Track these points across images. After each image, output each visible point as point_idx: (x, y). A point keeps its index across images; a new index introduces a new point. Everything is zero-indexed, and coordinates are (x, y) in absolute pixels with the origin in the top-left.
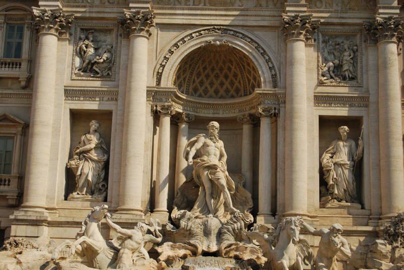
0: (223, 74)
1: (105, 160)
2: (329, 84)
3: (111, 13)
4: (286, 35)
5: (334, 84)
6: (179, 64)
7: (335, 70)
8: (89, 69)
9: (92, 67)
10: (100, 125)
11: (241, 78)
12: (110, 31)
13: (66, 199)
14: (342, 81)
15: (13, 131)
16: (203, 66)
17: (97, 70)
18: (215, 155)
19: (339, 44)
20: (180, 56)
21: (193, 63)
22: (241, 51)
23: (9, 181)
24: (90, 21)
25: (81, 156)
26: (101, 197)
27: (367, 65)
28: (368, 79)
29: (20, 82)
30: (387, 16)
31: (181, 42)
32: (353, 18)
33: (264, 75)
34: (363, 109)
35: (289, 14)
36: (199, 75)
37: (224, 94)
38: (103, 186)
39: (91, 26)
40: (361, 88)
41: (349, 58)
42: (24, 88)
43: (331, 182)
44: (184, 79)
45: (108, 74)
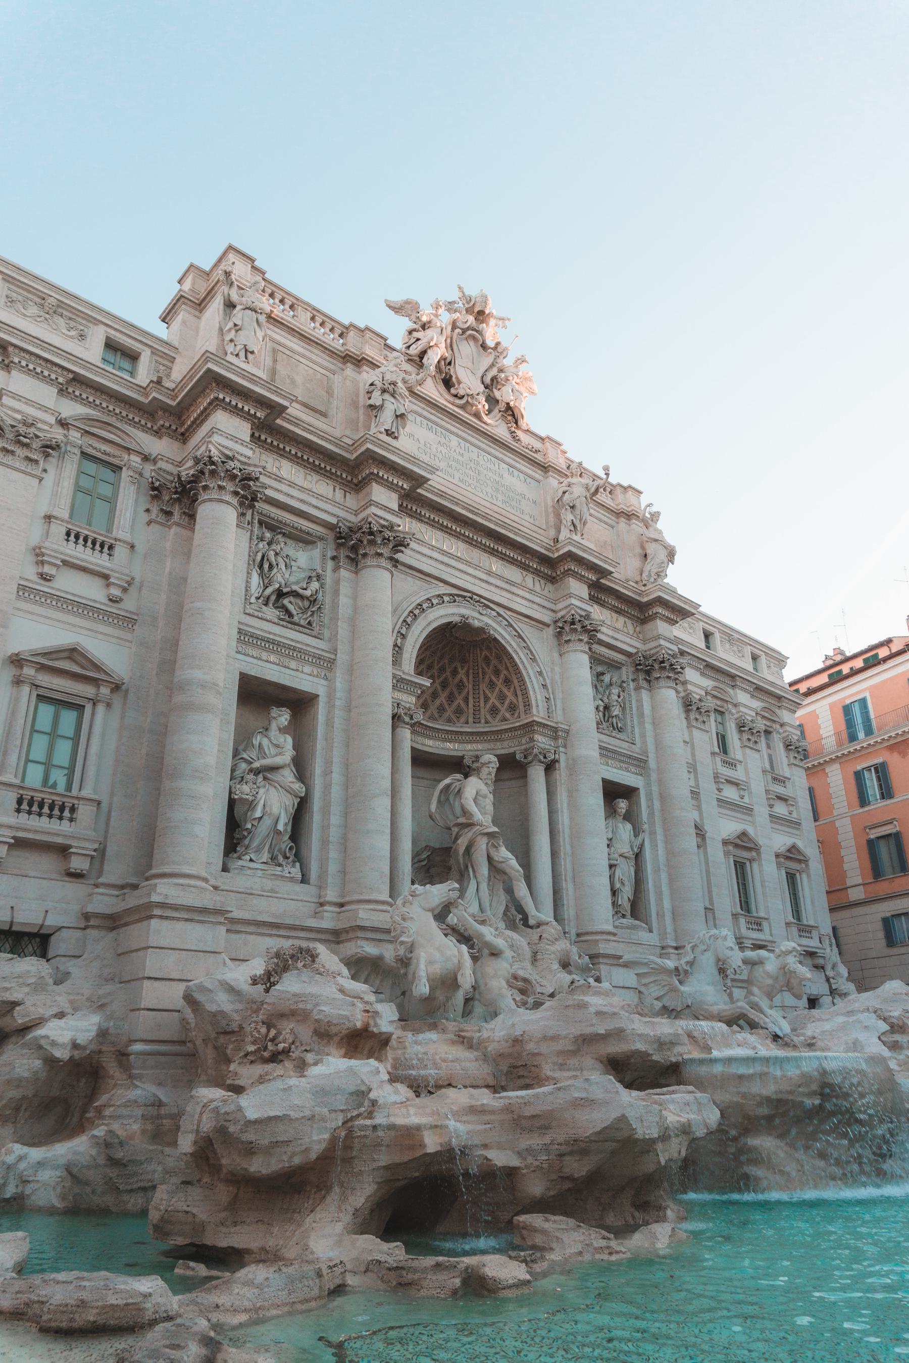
1: (303, 795)
13: (225, 869)
15: (89, 690)
17: (291, 608)
19: (603, 674)
22: (503, 646)
23: (73, 809)
25: (260, 777)
26: (296, 871)
27: (641, 715)
28: (643, 736)
29: (108, 585)
30: (670, 652)
32: (624, 643)
33: (536, 695)
34: (639, 777)
38: (291, 848)
39: (281, 522)
41: (620, 700)
42: (113, 600)
45: (310, 623)
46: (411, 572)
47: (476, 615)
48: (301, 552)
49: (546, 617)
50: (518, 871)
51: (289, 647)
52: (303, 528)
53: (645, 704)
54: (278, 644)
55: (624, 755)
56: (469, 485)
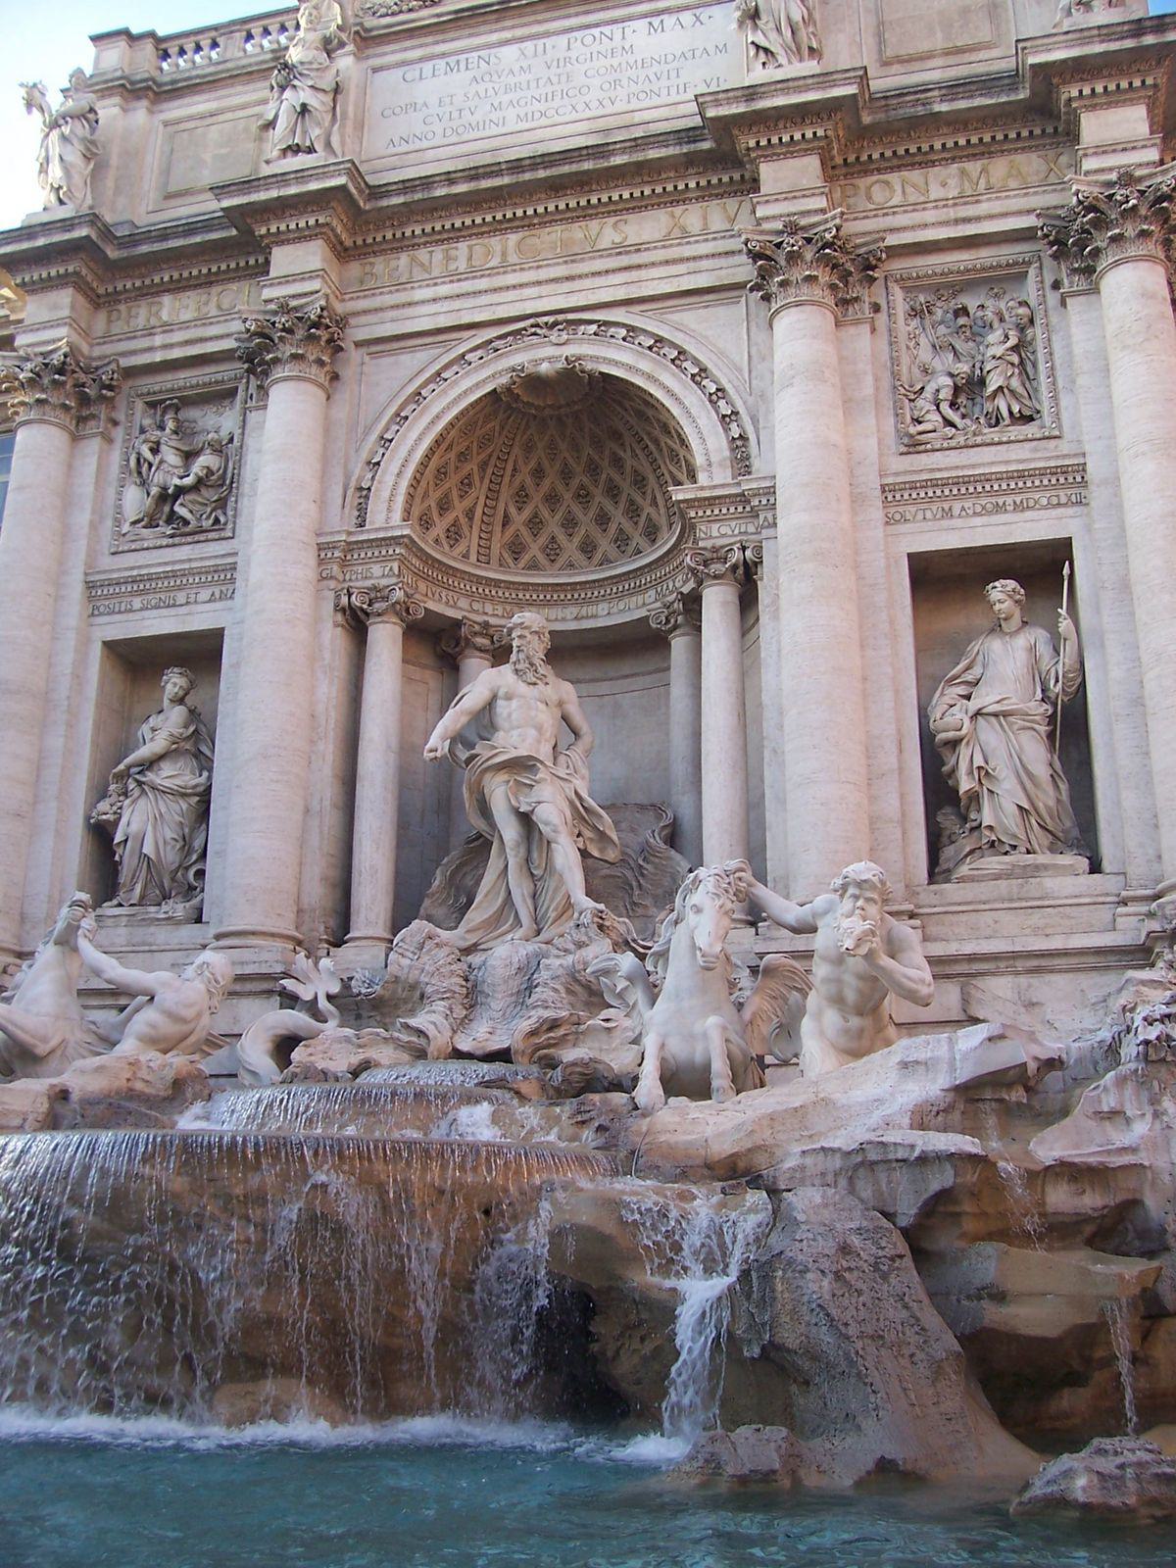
0: (602, 483)
1: (200, 789)
2: (938, 446)
3: (222, 337)
4: (766, 298)
5: (961, 440)
6: (432, 451)
7: (962, 400)
8: (164, 517)
9: (172, 511)
10: (192, 685)
11: (656, 487)
12: (232, 393)
14: (986, 430)
16: (532, 464)
18: (539, 729)
20: (427, 428)
21: (490, 456)
24: (169, 376)
25: (132, 785)
31: (432, 386)
33: (705, 440)
34: (1070, 511)
35: (766, 226)
36: (521, 497)
37: (612, 551)
40: (1052, 443)
43: (965, 785)
44: (470, 514)
45: (217, 521)
46: (402, 344)
47: (550, 351)
48: (228, 413)
49: (744, 270)
50: (547, 824)
51: (167, 576)
52: (207, 379)
53: (1074, 330)
54: (150, 578)
55: (999, 477)
56: (543, 114)
